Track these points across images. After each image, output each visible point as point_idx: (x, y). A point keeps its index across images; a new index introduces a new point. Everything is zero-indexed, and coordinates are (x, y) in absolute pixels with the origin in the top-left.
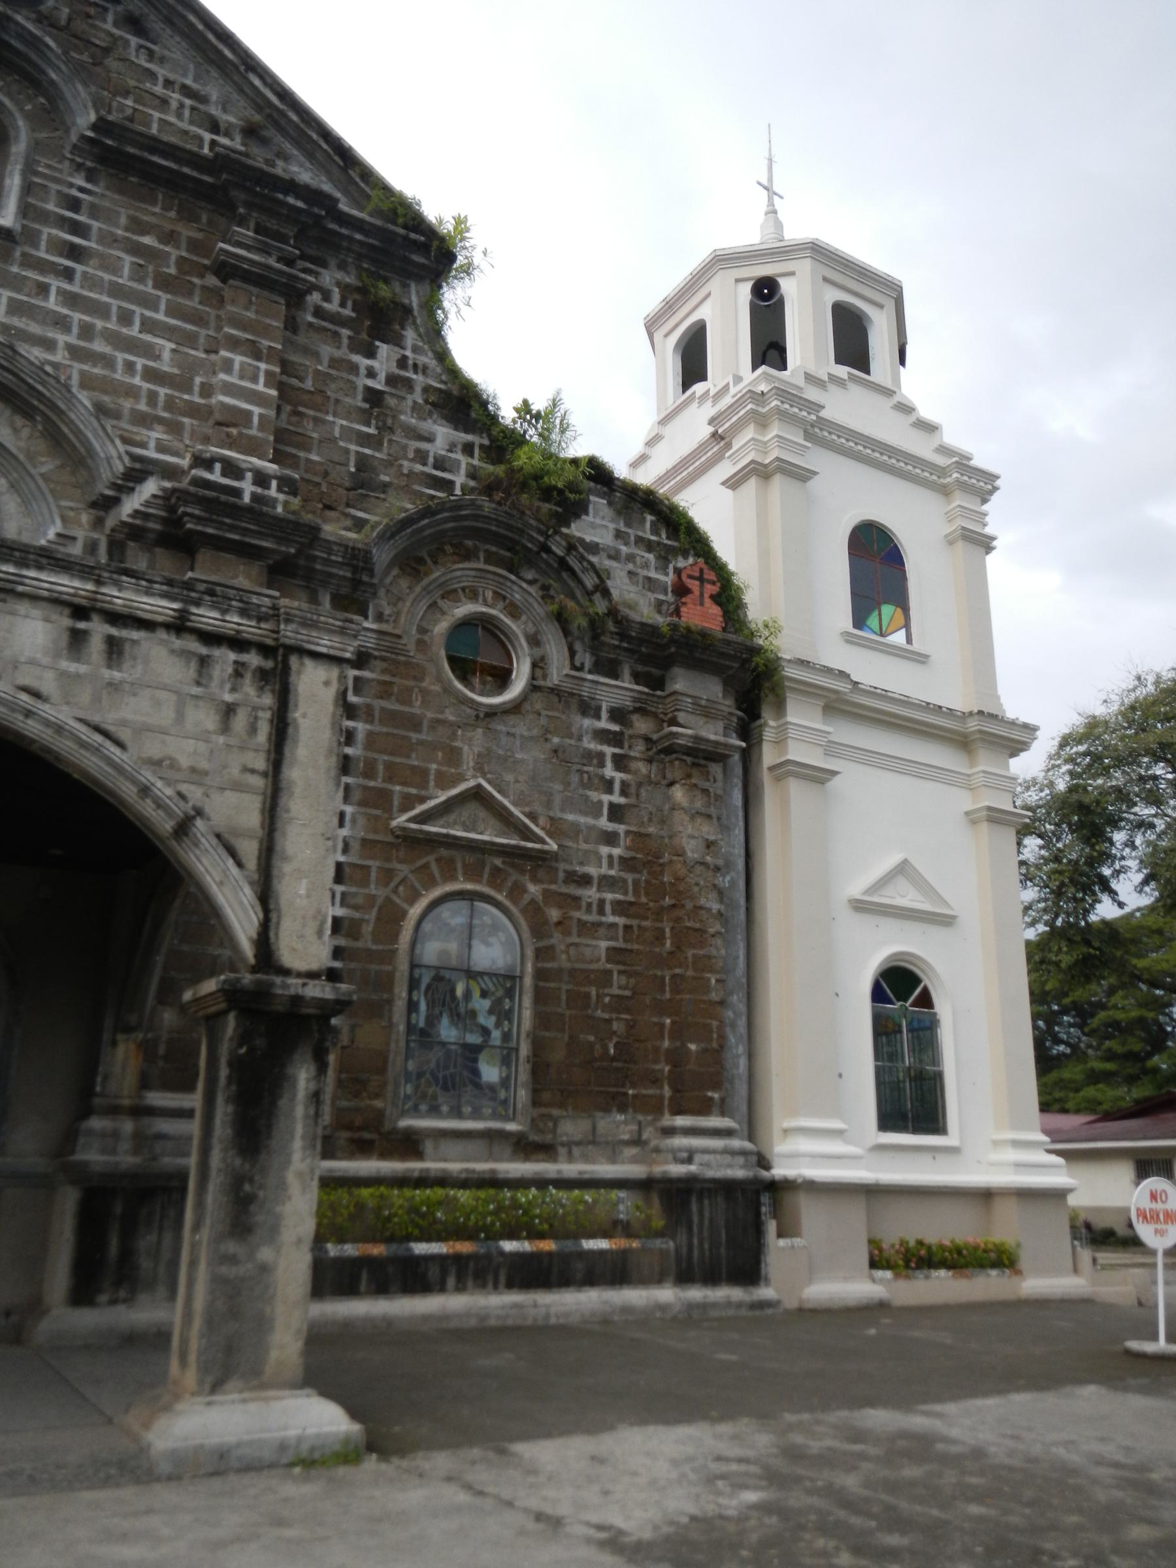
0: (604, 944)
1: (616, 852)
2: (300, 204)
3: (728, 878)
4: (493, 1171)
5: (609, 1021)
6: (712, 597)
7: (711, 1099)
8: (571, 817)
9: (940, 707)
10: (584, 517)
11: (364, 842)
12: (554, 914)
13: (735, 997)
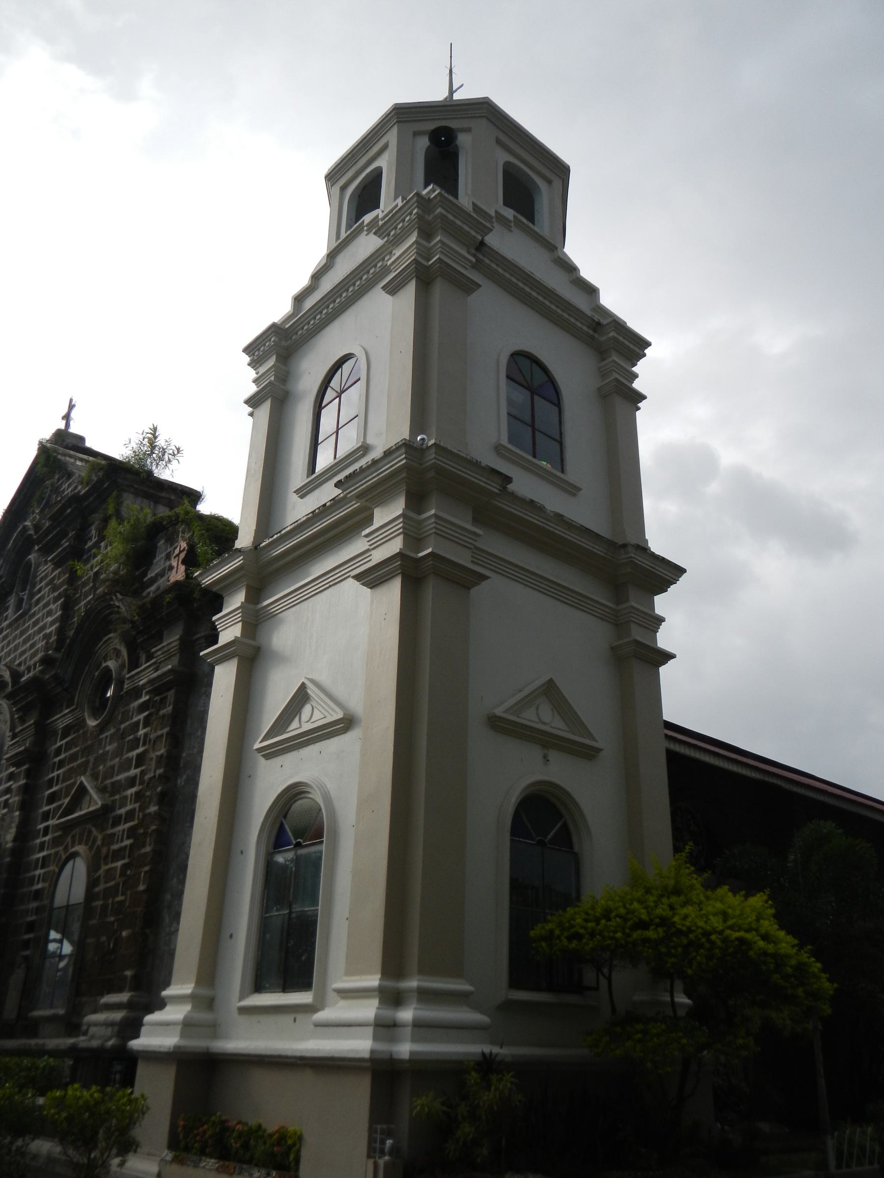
0: (119, 864)
1: (133, 790)
2: (69, 510)
3: (184, 777)
4: (44, 1045)
5: (114, 922)
6: (183, 562)
7: (126, 977)
8: (119, 778)
9: (325, 505)
10: (155, 561)
11: (54, 839)
12: (104, 850)
13: (175, 880)
